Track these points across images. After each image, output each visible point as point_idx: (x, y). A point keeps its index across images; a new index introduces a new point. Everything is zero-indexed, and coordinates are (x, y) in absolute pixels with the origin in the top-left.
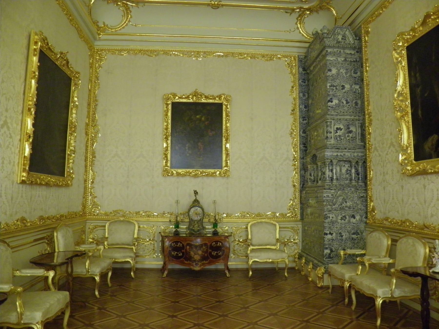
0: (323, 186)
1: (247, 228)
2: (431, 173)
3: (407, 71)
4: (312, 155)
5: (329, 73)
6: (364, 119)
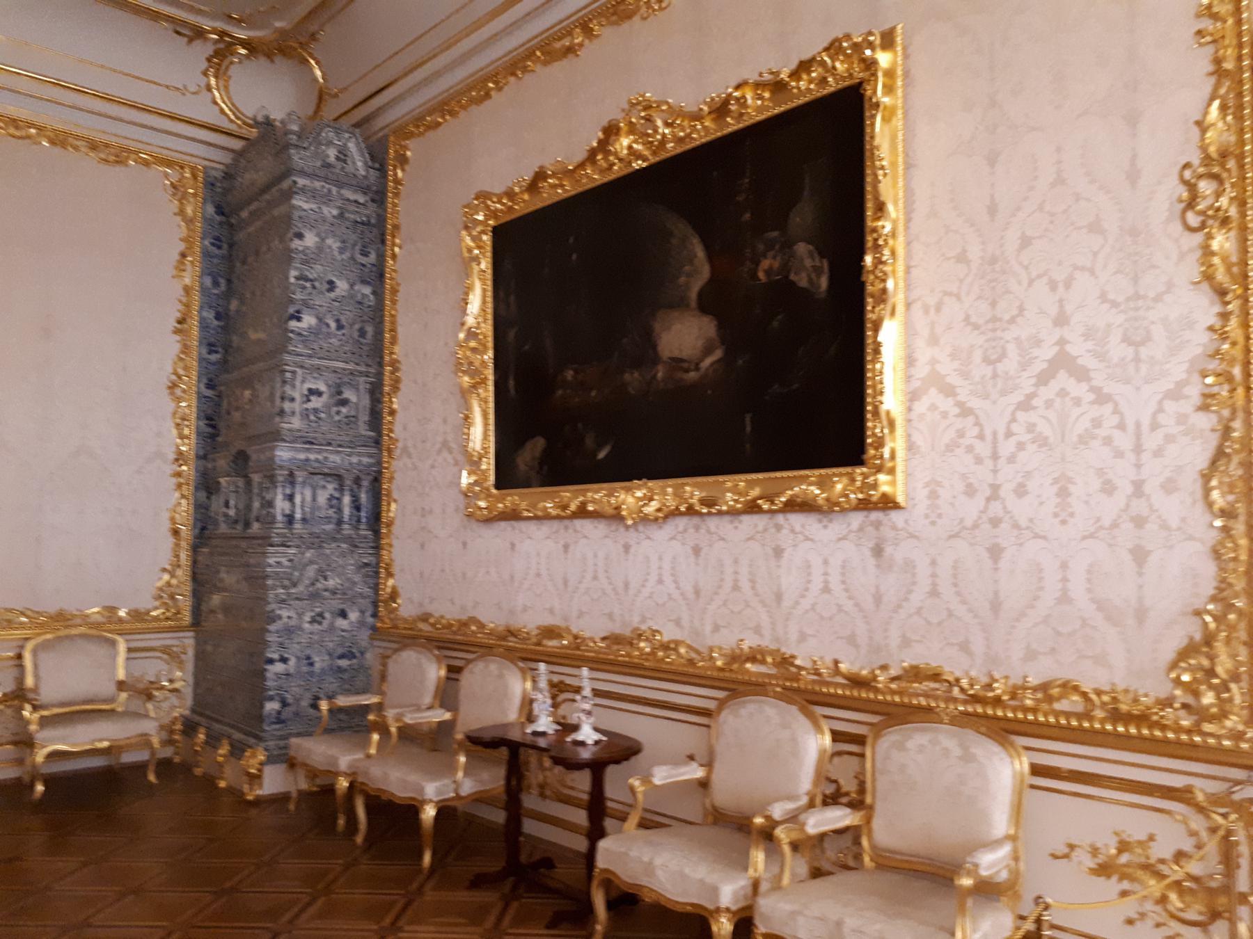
0: (263, 538)
1: (19, 656)
2: (529, 518)
3: (489, 283)
4: (234, 451)
5: (296, 243)
6: (380, 375)
